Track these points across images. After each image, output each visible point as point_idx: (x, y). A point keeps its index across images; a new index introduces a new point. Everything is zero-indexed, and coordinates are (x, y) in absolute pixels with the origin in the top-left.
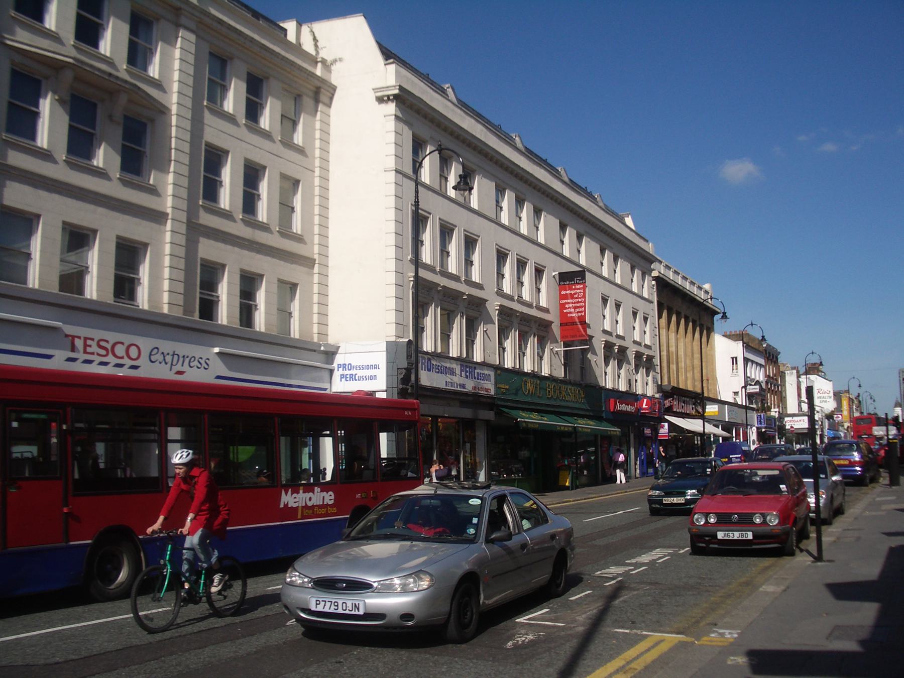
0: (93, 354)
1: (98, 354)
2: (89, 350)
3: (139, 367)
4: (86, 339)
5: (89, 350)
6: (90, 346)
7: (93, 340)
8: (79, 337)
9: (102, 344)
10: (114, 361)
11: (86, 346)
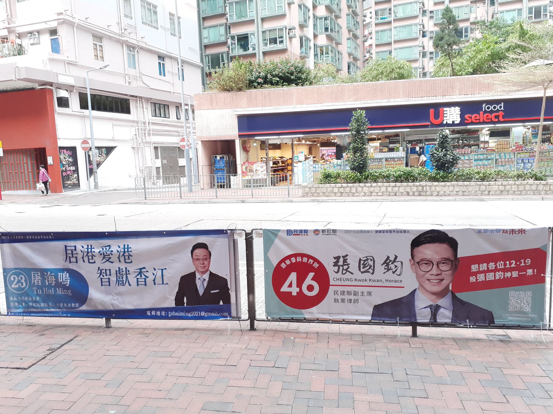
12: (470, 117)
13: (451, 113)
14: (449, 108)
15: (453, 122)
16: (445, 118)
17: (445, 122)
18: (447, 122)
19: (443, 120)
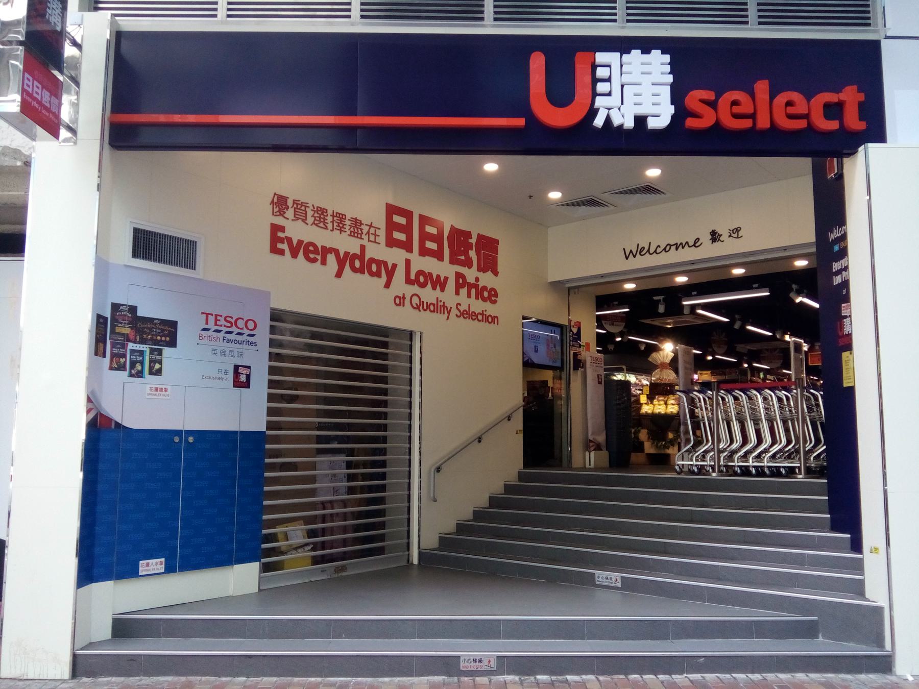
0: (221, 326)
1: (225, 326)
2: (218, 323)
3: (255, 335)
4: (216, 316)
5: (218, 323)
6: (219, 320)
7: (221, 316)
8: (212, 315)
9: (228, 319)
10: (236, 330)
11: (216, 320)
12: (713, 104)
13: (626, 79)
14: (618, 54)
15: (640, 121)
16: (600, 102)
17: (599, 122)
18: (608, 120)
19: (593, 112)
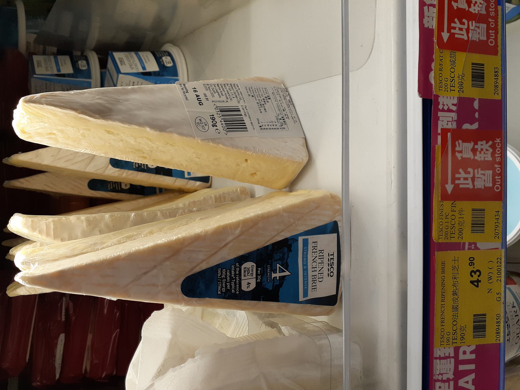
0: (331, 261)
1: (331, 263)
2: (331, 260)
4: (333, 258)
5: (331, 260)
6: (332, 260)
7: (333, 261)
8: (333, 257)
